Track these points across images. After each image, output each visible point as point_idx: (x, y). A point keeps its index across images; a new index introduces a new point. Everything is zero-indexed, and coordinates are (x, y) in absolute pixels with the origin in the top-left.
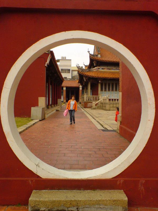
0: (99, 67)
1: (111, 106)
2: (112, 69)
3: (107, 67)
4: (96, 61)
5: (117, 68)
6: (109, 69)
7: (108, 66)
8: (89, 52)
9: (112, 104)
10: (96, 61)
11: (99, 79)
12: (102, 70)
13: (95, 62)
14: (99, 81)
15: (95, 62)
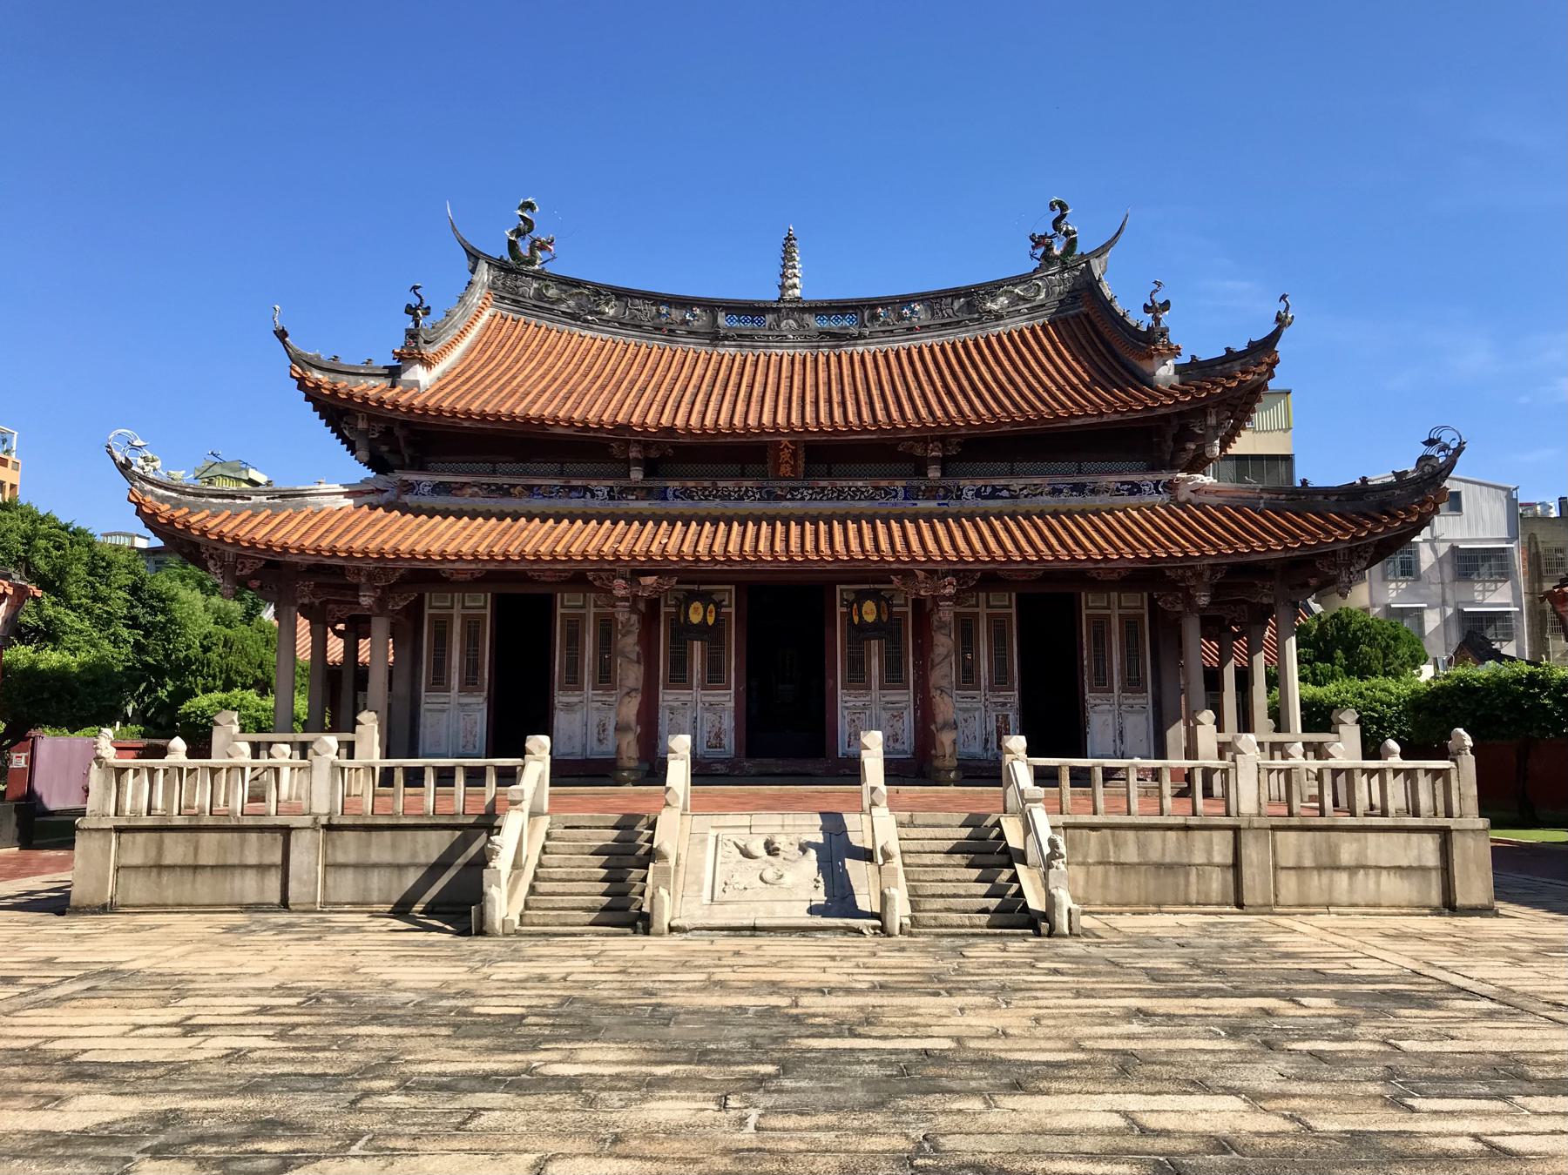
0: (412, 477)
1: (136, 858)
2: (530, 490)
3: (494, 472)
4: (371, 418)
5: (574, 483)
6: (499, 487)
7: (501, 467)
8: (286, 335)
9: (141, 838)
10: (371, 418)
11: (358, 570)
12: (441, 501)
13: (362, 425)
14: (355, 588)
15: (362, 425)
